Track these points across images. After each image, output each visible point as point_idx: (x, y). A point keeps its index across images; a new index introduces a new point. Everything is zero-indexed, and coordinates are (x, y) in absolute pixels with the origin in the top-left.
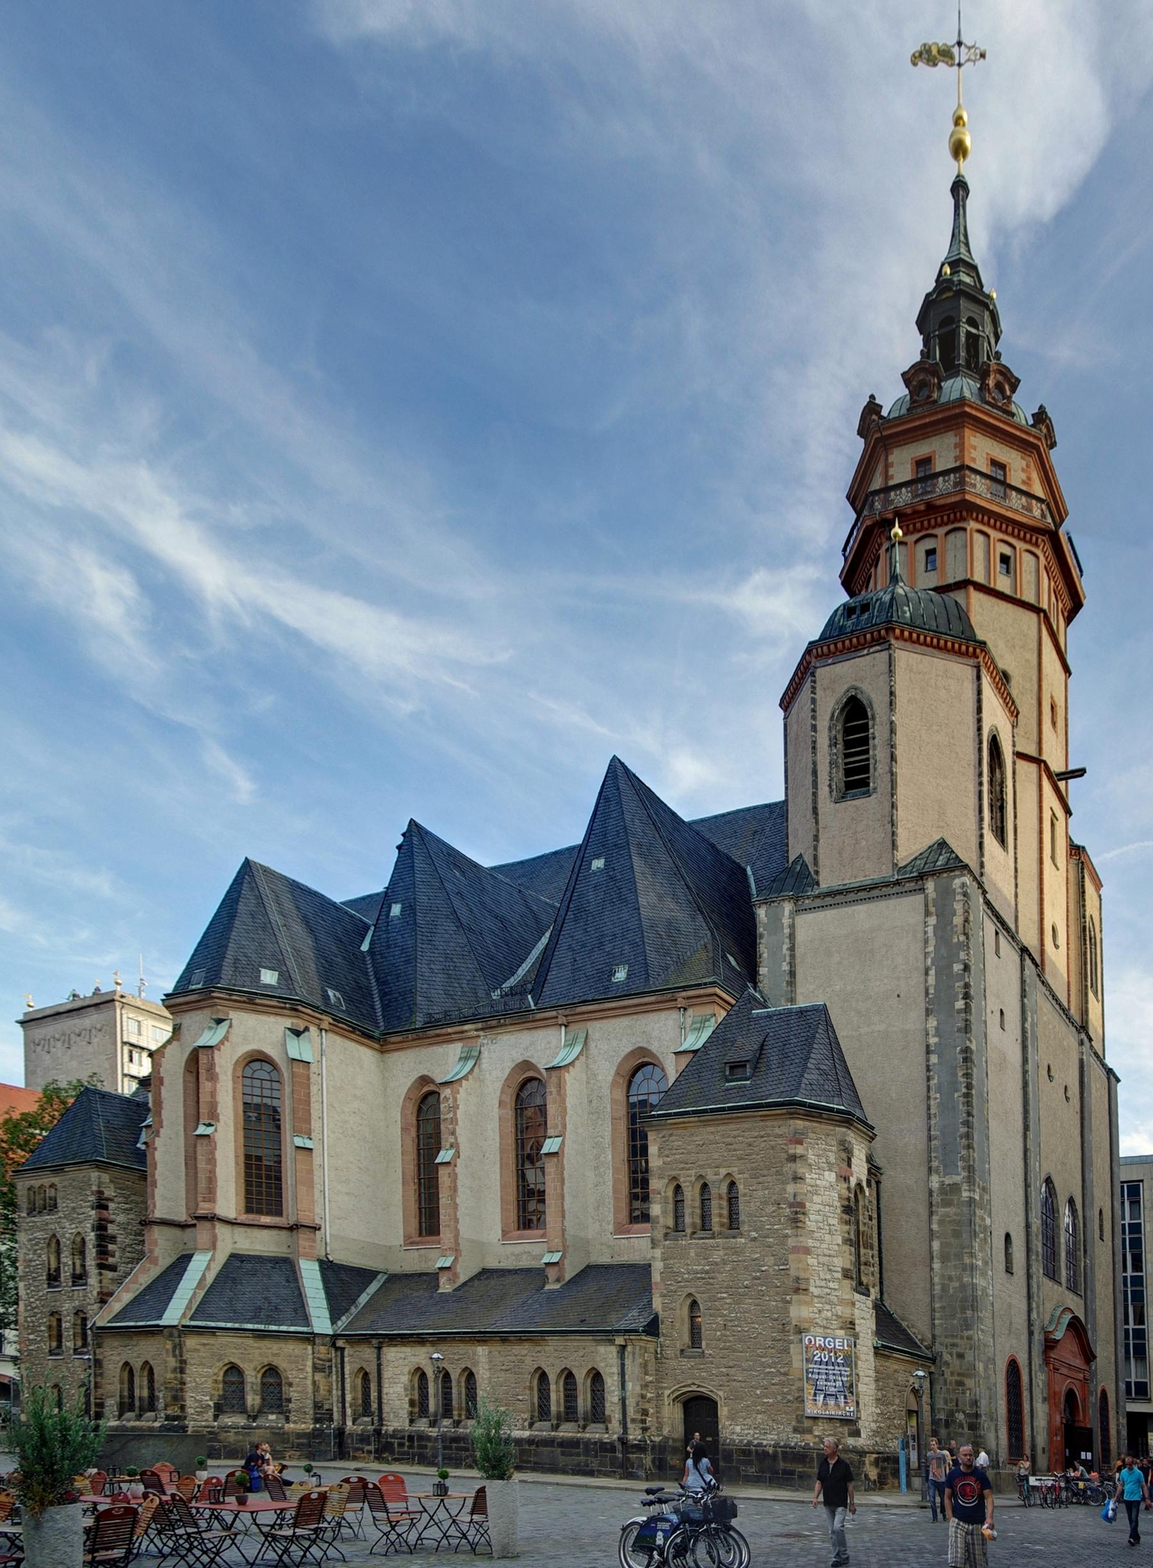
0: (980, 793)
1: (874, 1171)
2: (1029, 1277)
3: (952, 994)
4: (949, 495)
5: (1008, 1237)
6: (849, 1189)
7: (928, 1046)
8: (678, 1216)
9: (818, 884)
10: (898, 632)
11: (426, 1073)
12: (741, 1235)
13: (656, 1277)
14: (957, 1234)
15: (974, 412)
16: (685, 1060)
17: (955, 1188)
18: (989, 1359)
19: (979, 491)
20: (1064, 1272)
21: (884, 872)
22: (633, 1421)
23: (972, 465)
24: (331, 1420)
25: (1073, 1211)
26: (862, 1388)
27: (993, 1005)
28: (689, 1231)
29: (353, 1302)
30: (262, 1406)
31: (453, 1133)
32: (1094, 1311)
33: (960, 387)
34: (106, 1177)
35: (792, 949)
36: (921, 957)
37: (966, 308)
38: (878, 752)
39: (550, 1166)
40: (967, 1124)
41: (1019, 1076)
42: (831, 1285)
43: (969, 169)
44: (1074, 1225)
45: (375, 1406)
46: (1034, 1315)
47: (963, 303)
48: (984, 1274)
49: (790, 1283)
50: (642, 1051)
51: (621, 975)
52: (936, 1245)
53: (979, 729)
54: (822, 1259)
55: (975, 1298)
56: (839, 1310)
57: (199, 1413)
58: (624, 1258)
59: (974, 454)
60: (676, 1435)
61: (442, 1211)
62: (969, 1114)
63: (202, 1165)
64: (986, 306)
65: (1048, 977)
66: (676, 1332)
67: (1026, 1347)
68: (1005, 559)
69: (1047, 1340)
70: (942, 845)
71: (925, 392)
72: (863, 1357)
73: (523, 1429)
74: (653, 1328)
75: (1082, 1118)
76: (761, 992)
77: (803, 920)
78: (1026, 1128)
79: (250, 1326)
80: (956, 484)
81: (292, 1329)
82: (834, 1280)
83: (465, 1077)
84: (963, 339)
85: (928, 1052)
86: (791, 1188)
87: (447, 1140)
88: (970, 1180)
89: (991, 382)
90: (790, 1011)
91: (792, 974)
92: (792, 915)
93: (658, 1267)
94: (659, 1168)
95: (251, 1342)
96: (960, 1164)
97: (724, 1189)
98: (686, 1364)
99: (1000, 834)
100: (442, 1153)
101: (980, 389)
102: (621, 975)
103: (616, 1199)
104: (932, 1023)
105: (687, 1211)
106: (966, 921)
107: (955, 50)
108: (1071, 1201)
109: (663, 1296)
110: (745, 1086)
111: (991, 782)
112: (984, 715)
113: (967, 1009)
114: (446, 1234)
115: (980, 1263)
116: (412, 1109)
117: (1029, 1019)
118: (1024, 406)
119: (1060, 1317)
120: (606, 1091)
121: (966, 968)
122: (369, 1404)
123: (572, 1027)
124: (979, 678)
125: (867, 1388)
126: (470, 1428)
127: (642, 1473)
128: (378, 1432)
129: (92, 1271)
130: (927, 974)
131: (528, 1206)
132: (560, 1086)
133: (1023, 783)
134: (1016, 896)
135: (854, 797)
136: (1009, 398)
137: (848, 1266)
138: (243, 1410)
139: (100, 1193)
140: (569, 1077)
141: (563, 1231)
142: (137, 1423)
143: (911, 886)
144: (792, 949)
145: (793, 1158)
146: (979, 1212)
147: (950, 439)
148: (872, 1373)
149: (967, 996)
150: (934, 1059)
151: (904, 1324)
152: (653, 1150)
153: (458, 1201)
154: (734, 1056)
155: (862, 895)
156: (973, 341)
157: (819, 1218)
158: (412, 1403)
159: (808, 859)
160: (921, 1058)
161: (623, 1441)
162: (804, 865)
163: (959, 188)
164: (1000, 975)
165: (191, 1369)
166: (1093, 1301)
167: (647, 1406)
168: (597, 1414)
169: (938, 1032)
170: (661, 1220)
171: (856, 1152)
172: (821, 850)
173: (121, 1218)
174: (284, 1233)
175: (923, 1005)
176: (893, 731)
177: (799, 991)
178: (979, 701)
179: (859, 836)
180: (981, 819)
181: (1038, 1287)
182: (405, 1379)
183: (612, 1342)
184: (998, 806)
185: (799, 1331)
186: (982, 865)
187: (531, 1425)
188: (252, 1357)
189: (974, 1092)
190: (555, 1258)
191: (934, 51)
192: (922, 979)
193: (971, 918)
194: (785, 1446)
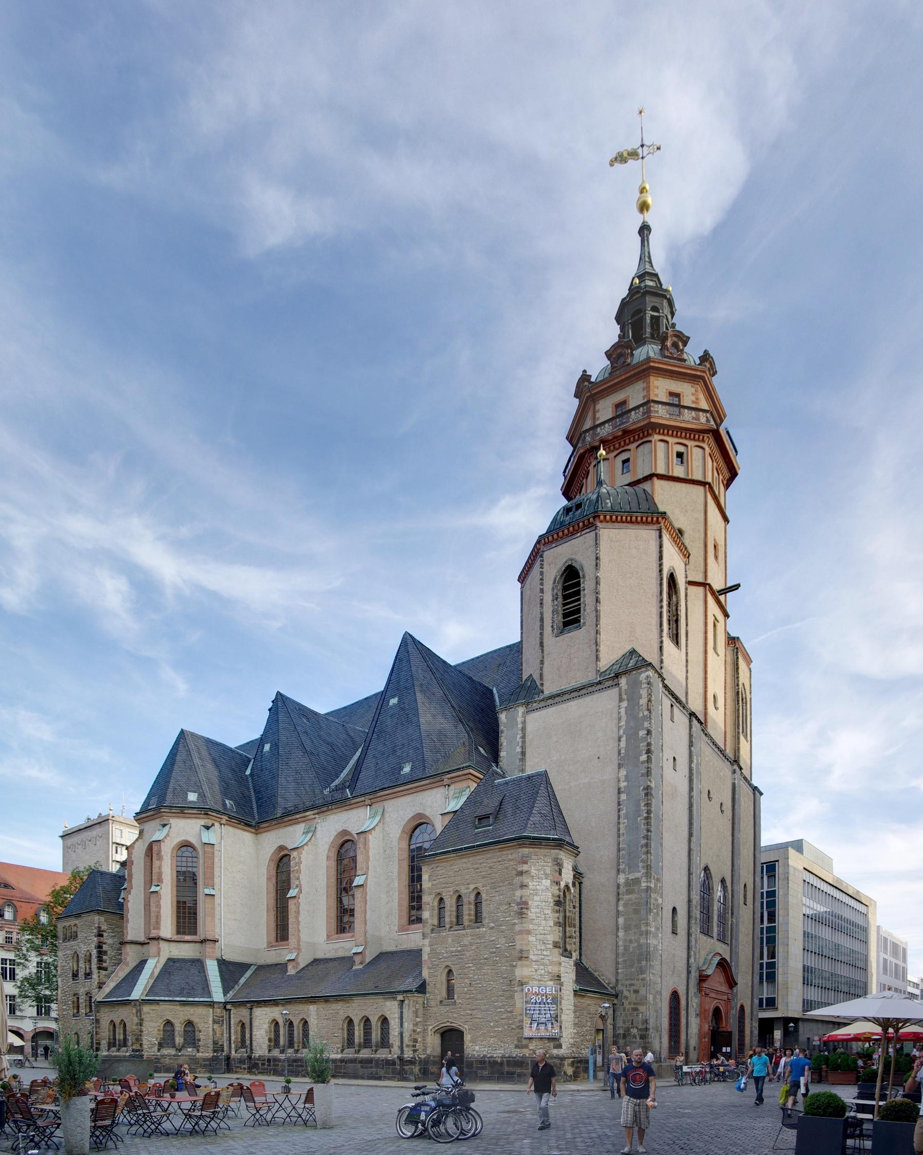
0: (661, 613)
1: (578, 875)
2: (689, 935)
3: (638, 752)
4: (639, 421)
5: (674, 909)
6: (559, 889)
7: (619, 789)
8: (441, 917)
9: (542, 692)
10: (602, 517)
11: (282, 844)
12: (483, 926)
13: (425, 957)
15: (657, 365)
16: (448, 818)
17: (637, 881)
18: (657, 992)
19: (661, 414)
20: (715, 929)
21: (592, 677)
22: (408, 1046)
23: (656, 399)
24: (223, 1051)
25: (724, 887)
26: (564, 1017)
27: (668, 755)
28: (448, 926)
29: (237, 982)
30: (184, 1043)
31: (298, 879)
32: (737, 953)
33: (649, 351)
34: (102, 919)
35: (523, 737)
36: (616, 730)
37: (650, 301)
38: (587, 598)
39: (358, 894)
41: (687, 800)
42: (545, 953)
43: (650, 217)
44: (725, 897)
45: (248, 1042)
46: (692, 960)
47: (648, 298)
48: (656, 936)
49: (516, 954)
50: (420, 815)
51: (407, 769)
53: (661, 571)
55: (648, 953)
56: (550, 968)
57: (150, 1048)
58: (404, 947)
59: (657, 391)
60: (435, 1054)
61: (290, 926)
62: (648, 831)
63: (153, 909)
64: (665, 297)
65: (710, 730)
66: (437, 989)
67: (685, 982)
68: (680, 455)
69: (700, 976)
70: (633, 652)
71: (622, 360)
72: (565, 997)
73: (337, 1053)
74: (422, 988)
75: (733, 823)
76: (501, 768)
77: (531, 717)
78: (691, 835)
79: (178, 999)
80: (644, 413)
81: (201, 999)
82: (547, 949)
83: (306, 844)
84: (648, 321)
86: (518, 893)
87: (294, 882)
88: (648, 875)
89: (669, 343)
90: (521, 779)
91: (523, 753)
92: (524, 716)
94: (429, 888)
95: (178, 1008)
96: (641, 864)
97: (472, 897)
98: (443, 1009)
99: (676, 639)
100: (291, 891)
101: (661, 349)
102: (407, 769)
103: (400, 911)
104: (623, 772)
105: (447, 914)
106: (649, 701)
107: (640, 151)
108: (723, 881)
109: (429, 968)
110: (488, 830)
111: (669, 604)
112: (665, 561)
113: (649, 760)
114: (292, 940)
115: (653, 929)
116: (273, 866)
117: (695, 761)
118: (692, 354)
119: (711, 959)
120: (395, 843)
121: (649, 732)
122: (245, 1042)
123: (374, 806)
124: (660, 537)
125: (568, 1017)
126: (305, 1054)
127: (412, 1077)
128: (250, 1057)
130: (619, 740)
131: (344, 919)
132: (366, 843)
133: (693, 604)
134: (687, 678)
136: (682, 350)
137: (557, 940)
138: (174, 1046)
139: (99, 927)
140: (371, 837)
141: (365, 932)
142: (117, 1054)
143: (610, 683)
144: (523, 737)
145: (521, 873)
147: (640, 385)
148: (572, 1008)
149: (649, 751)
150: (623, 797)
152: (425, 877)
153: (300, 919)
154: (481, 812)
155: (573, 695)
156: (656, 321)
157: (538, 910)
158: (270, 1040)
159: (536, 677)
161: (401, 1059)
162: (533, 681)
163: (644, 230)
164: (673, 733)
165: (145, 1024)
166: (737, 946)
167: (416, 1037)
168: (385, 1042)
169: (627, 778)
170: (430, 921)
171: (565, 865)
172: (545, 670)
173: (110, 941)
174: (198, 945)
175: (616, 762)
176: (597, 583)
178: (661, 552)
179: (572, 656)
180: (662, 631)
181: (696, 941)
182: (266, 1026)
183: (395, 999)
184: (675, 620)
185: (521, 984)
186: (662, 661)
187: (342, 1051)
188: (179, 1016)
190: (360, 949)
191: (625, 154)
192: (616, 744)
193: (653, 699)
194: (509, 1057)
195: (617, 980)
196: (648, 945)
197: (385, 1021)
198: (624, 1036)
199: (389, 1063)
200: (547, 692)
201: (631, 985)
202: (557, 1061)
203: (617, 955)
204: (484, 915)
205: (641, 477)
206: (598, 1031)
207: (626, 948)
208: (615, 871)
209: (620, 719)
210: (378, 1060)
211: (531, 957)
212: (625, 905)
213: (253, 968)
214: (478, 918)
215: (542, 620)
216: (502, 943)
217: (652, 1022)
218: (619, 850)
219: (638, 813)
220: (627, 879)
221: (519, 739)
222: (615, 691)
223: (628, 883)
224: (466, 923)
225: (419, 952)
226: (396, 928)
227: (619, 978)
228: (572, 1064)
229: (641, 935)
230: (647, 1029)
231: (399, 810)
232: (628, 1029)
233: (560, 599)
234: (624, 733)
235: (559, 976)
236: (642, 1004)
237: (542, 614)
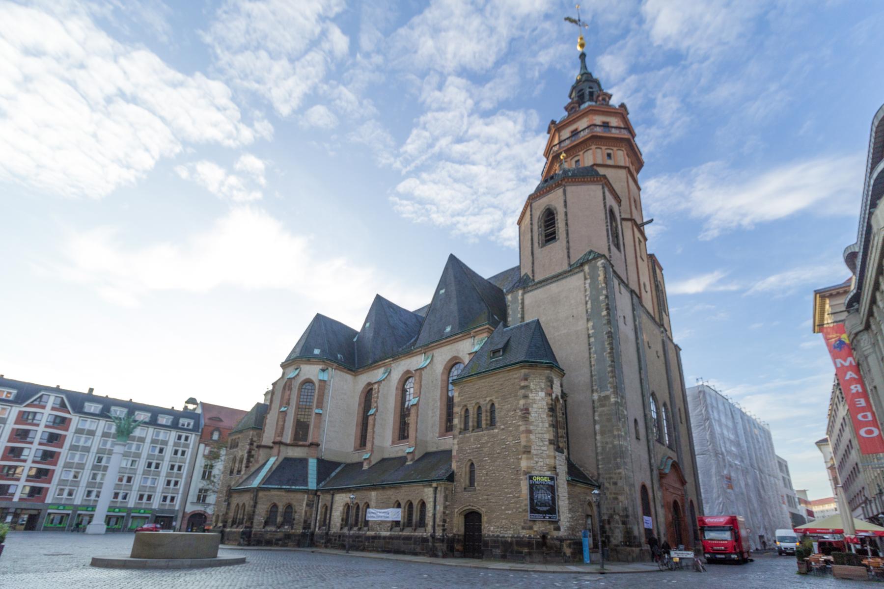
8: (466, 423)
13: (454, 453)
14: (609, 420)
17: (607, 398)
21: (566, 267)
22: (439, 526)
24: (310, 528)
27: (619, 313)
36: (583, 298)
48: (625, 439)
55: (622, 452)
62: (613, 361)
66: (462, 478)
72: (561, 486)
74: (451, 478)
85: (589, 336)
89: (600, 98)
96: (609, 385)
104: (591, 324)
109: (457, 462)
122: (326, 522)
127: (440, 554)
128: (327, 534)
129: (244, 469)
138: (275, 524)
146: (621, 408)
148: (566, 495)
150: (592, 340)
151: (582, 469)
158: (342, 520)
160: (586, 341)
164: (623, 302)
168: (422, 523)
169: (594, 327)
170: (458, 426)
175: (585, 318)
182: (341, 508)
183: (431, 486)
195: (599, 474)
196: (621, 446)
197: (423, 504)
198: (609, 523)
199: (424, 540)
200: (536, 280)
201: (610, 478)
202: (557, 543)
203: (597, 454)
204: (497, 419)
206: (588, 516)
207: (603, 448)
208: (590, 391)
209: (586, 291)
210: (416, 538)
212: (600, 416)
213: (342, 466)
214: (492, 423)
216: (510, 441)
217: (630, 509)
218: (592, 376)
219: (604, 350)
220: (600, 396)
221: (519, 309)
222: (582, 274)
223: (600, 399)
224: (484, 426)
225: (450, 451)
227: (601, 471)
228: (569, 546)
229: (615, 437)
230: (627, 516)
231: (442, 355)
232: (611, 516)
233: (543, 228)
236: (621, 494)
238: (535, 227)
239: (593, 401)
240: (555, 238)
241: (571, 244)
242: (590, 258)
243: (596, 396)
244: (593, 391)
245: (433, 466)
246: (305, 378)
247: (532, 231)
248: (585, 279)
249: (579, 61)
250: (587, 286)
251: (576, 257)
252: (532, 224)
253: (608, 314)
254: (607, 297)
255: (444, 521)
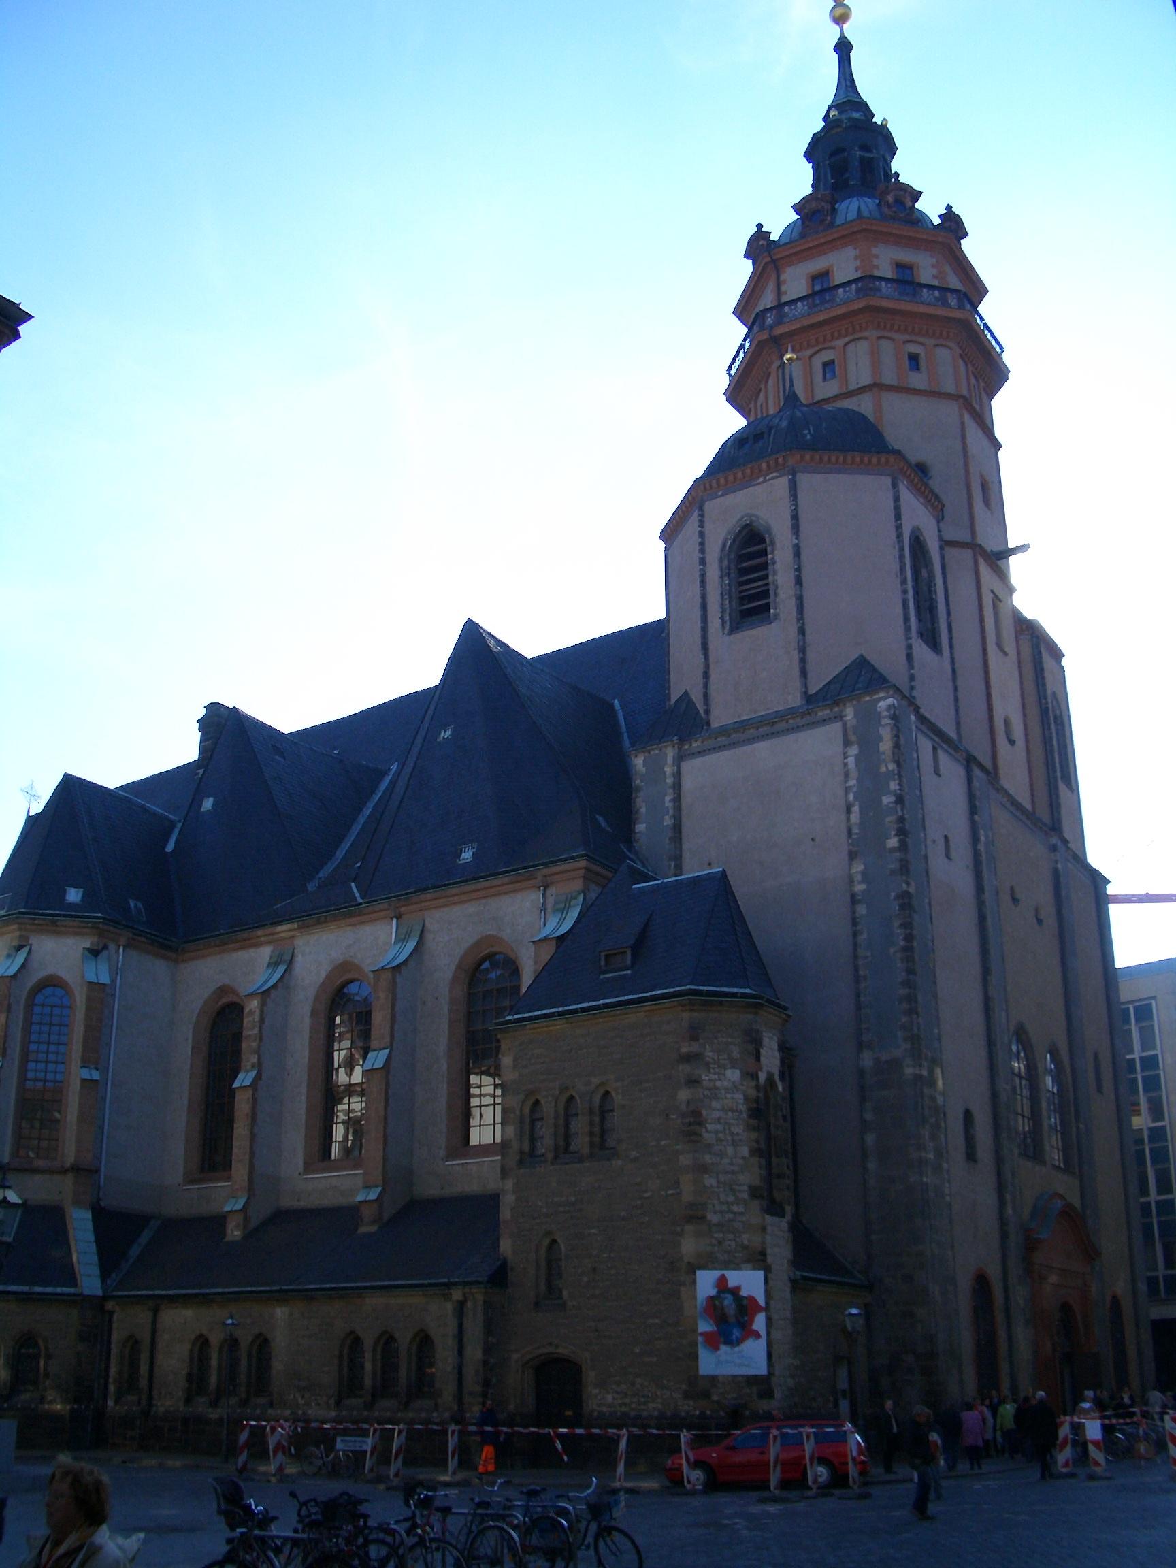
7: (853, 896)
13: (506, 1214)
23: (876, 273)
36: (841, 792)
40: (907, 984)
52: (870, 1139)
54: (722, 1178)
59: (875, 262)
62: (910, 972)
85: (854, 899)
93: (508, 1200)
96: (900, 1034)
101: (879, 205)
104: (858, 867)
130: (849, 811)
135: (753, 626)
148: (788, 1314)
150: (862, 910)
159: (697, 697)
162: (690, 703)
177: (685, 847)
183: (447, 1297)
186: (912, 678)
189: (915, 944)
192: (843, 817)
197: (424, 1341)
205: (853, 387)
209: (847, 775)
211: (710, 1216)
215: (704, 607)
218: (859, 1007)
222: (837, 726)
226: (442, 1153)
234: (856, 798)
235: (763, 1254)
237: (704, 597)
238: (713, 573)
239: (861, 1073)
240: (767, 608)
241: (809, 637)
242: (861, 677)
243: (867, 1059)
244: (860, 1046)
245: (431, 1229)
246: (42, 974)
247: (703, 582)
248: (847, 743)
249: (835, 57)
250: (851, 761)
251: (823, 674)
252: (703, 561)
253: (903, 846)
254: (900, 800)
255: (486, 1383)
